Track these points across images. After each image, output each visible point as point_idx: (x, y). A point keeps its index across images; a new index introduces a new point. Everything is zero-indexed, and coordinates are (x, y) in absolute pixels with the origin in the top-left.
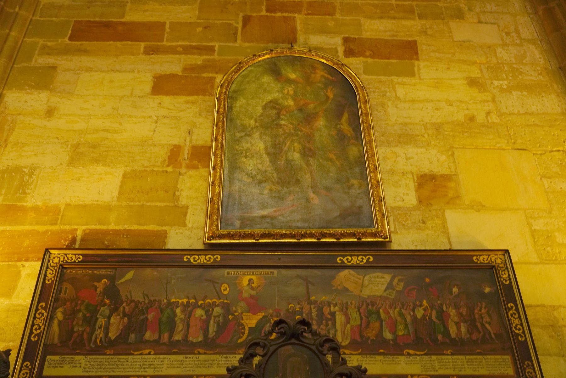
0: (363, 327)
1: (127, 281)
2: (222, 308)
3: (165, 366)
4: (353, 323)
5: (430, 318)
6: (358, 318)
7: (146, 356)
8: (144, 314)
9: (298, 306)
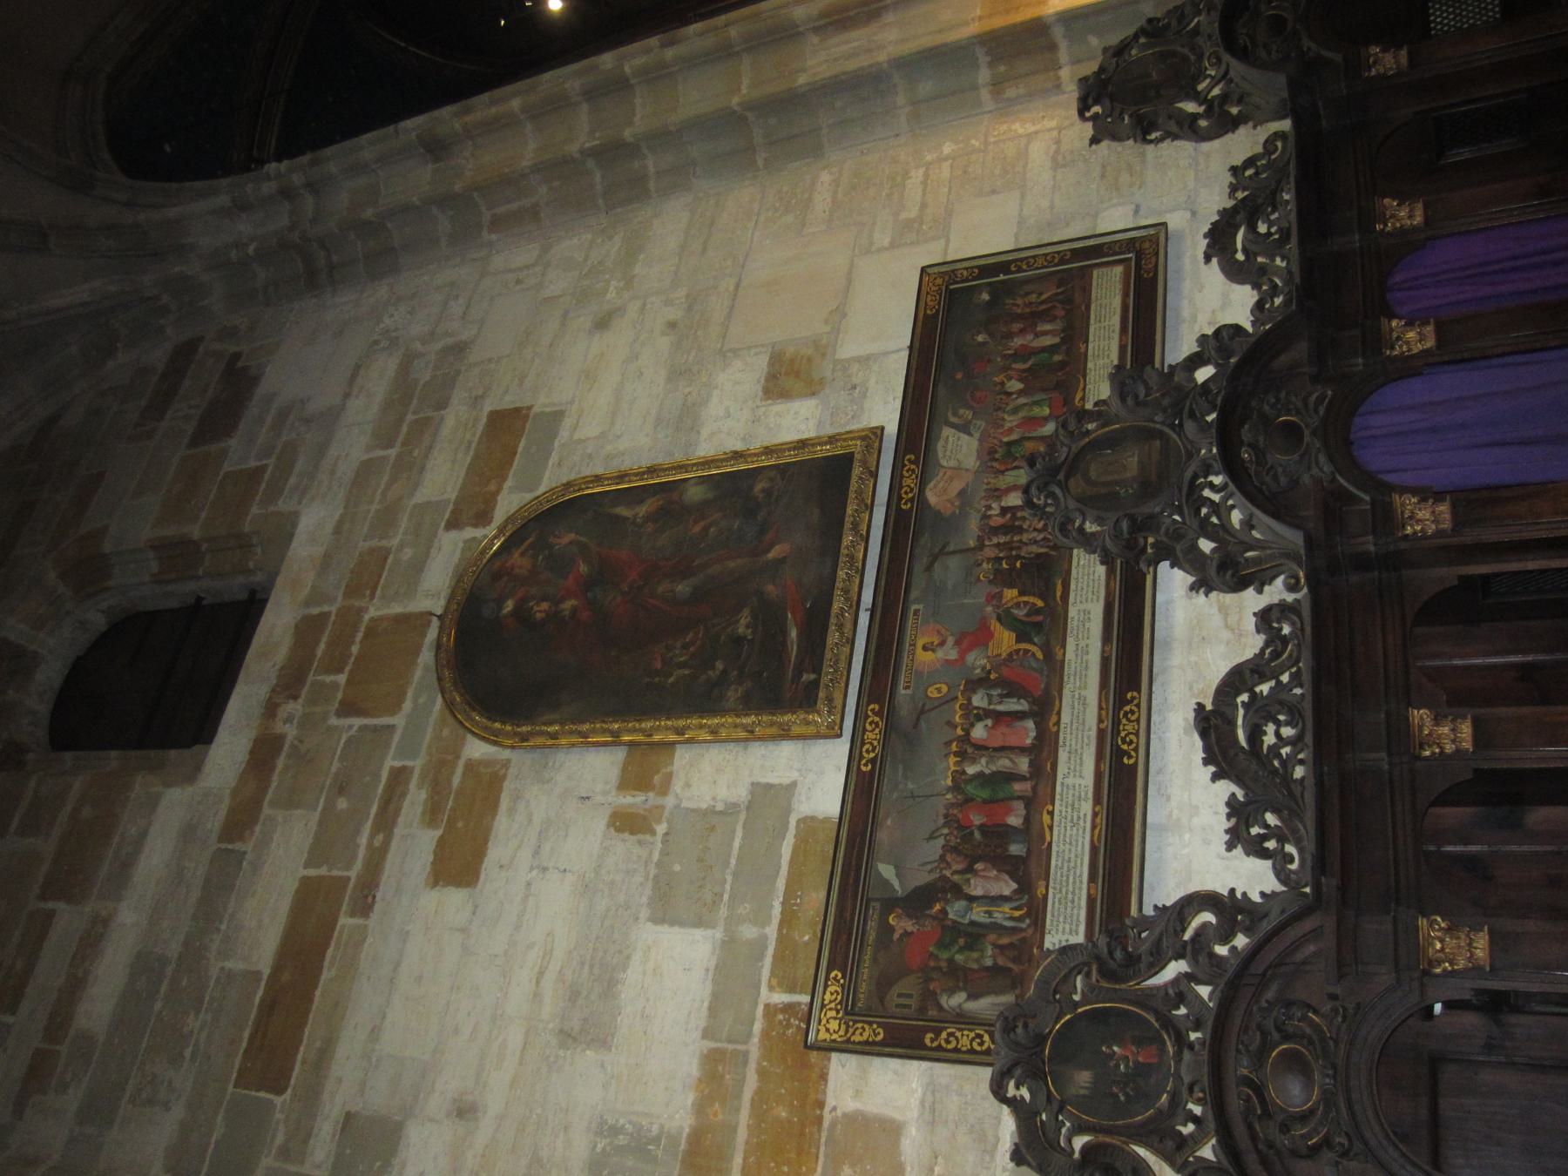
1: (898, 875)
2: (974, 692)
3: (1078, 781)
5: (1024, 371)
7: (1056, 818)
8: (972, 833)
9: (985, 565)
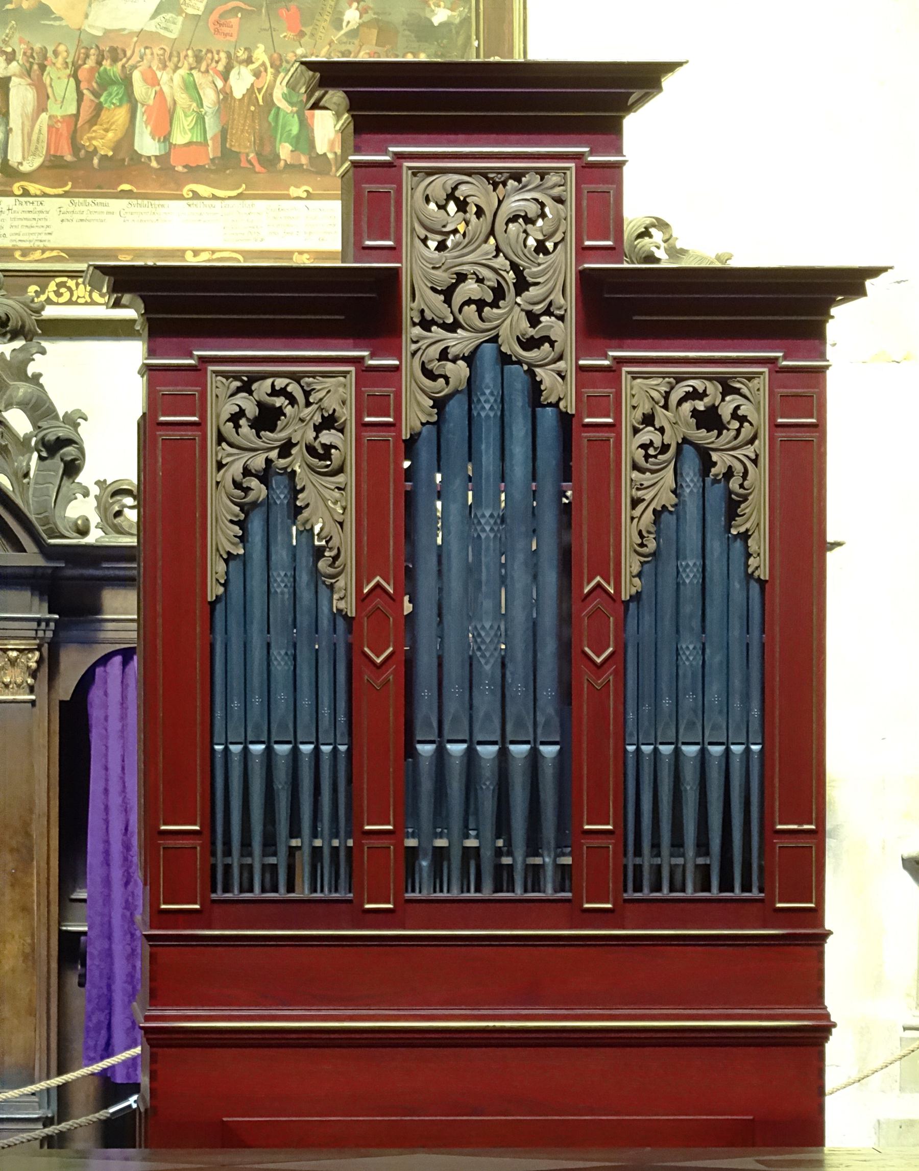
0: (80, 123)
4: (54, 109)
6: (72, 95)
